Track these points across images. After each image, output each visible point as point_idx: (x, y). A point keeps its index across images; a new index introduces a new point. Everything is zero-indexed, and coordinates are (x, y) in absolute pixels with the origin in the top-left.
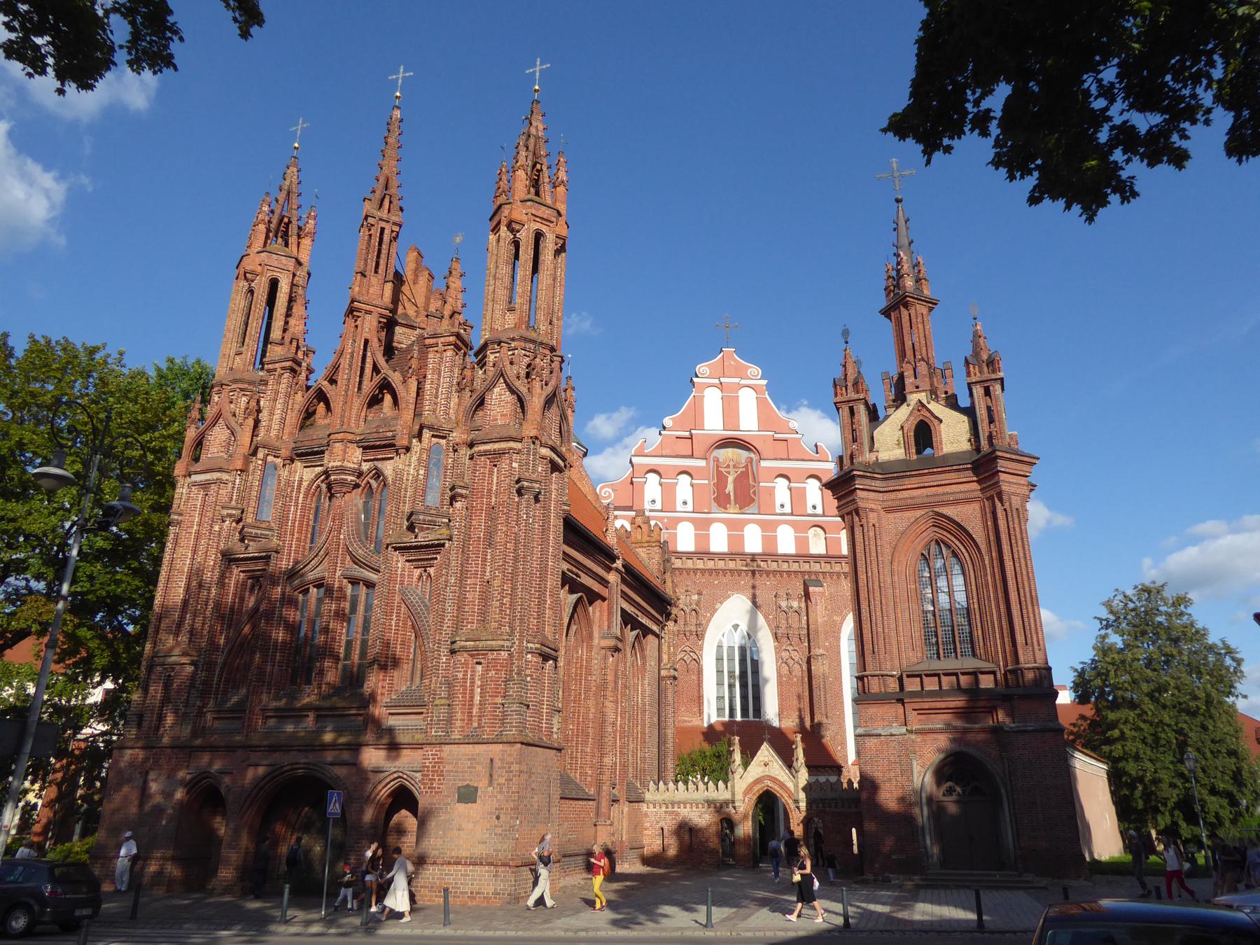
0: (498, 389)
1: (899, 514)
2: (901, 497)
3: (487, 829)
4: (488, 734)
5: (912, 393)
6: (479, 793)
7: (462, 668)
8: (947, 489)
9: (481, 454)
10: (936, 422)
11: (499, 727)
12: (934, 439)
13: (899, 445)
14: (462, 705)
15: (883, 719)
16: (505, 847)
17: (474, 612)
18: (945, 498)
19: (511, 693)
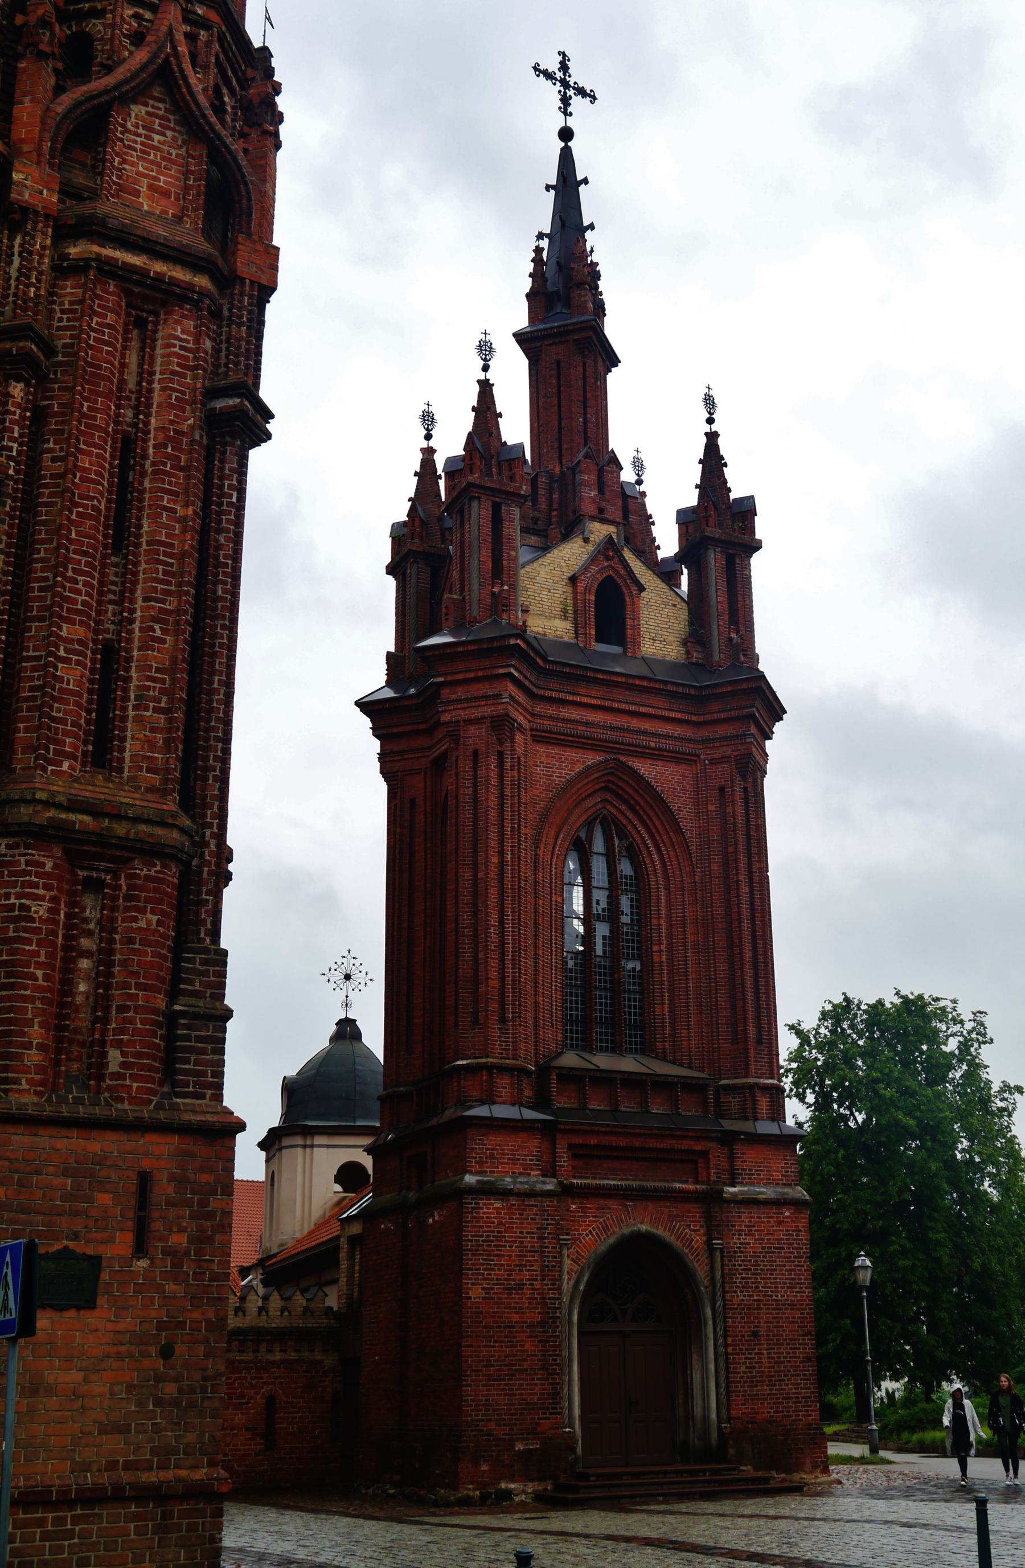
0: (143, 110)
1: (555, 751)
2: (567, 715)
3: (130, 1388)
4: (133, 1100)
5: (593, 518)
6: (105, 1276)
7: (46, 887)
8: (646, 725)
9: (108, 270)
10: (634, 589)
11: (161, 1084)
12: (629, 622)
13: (565, 611)
14: (43, 1000)
15: (514, 1161)
16: (191, 1438)
17: (79, 726)
18: (643, 741)
19: (197, 986)
